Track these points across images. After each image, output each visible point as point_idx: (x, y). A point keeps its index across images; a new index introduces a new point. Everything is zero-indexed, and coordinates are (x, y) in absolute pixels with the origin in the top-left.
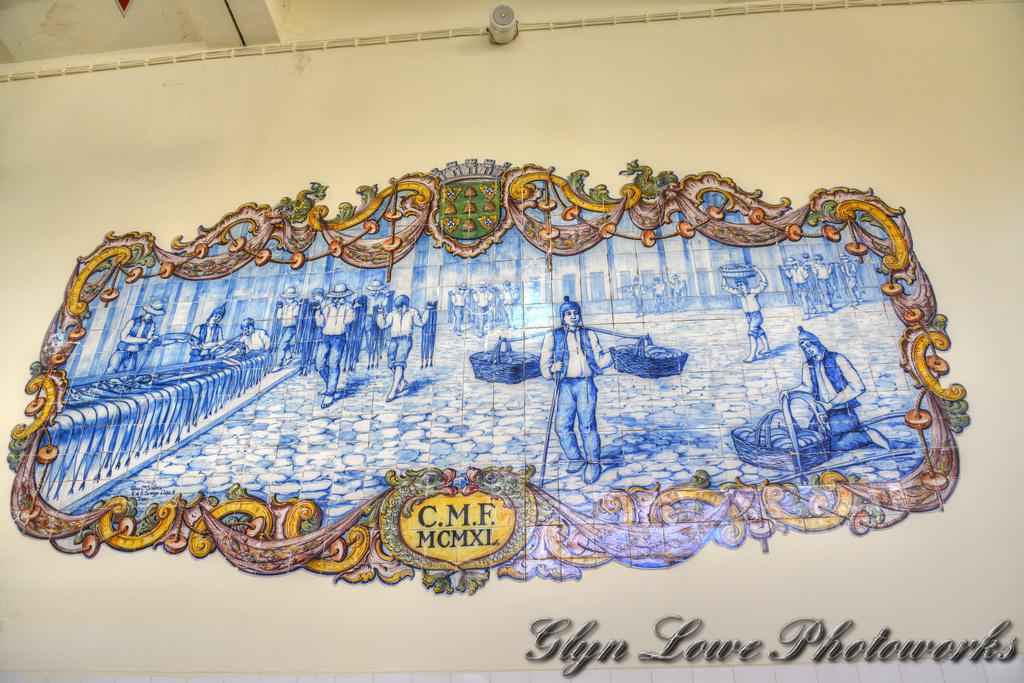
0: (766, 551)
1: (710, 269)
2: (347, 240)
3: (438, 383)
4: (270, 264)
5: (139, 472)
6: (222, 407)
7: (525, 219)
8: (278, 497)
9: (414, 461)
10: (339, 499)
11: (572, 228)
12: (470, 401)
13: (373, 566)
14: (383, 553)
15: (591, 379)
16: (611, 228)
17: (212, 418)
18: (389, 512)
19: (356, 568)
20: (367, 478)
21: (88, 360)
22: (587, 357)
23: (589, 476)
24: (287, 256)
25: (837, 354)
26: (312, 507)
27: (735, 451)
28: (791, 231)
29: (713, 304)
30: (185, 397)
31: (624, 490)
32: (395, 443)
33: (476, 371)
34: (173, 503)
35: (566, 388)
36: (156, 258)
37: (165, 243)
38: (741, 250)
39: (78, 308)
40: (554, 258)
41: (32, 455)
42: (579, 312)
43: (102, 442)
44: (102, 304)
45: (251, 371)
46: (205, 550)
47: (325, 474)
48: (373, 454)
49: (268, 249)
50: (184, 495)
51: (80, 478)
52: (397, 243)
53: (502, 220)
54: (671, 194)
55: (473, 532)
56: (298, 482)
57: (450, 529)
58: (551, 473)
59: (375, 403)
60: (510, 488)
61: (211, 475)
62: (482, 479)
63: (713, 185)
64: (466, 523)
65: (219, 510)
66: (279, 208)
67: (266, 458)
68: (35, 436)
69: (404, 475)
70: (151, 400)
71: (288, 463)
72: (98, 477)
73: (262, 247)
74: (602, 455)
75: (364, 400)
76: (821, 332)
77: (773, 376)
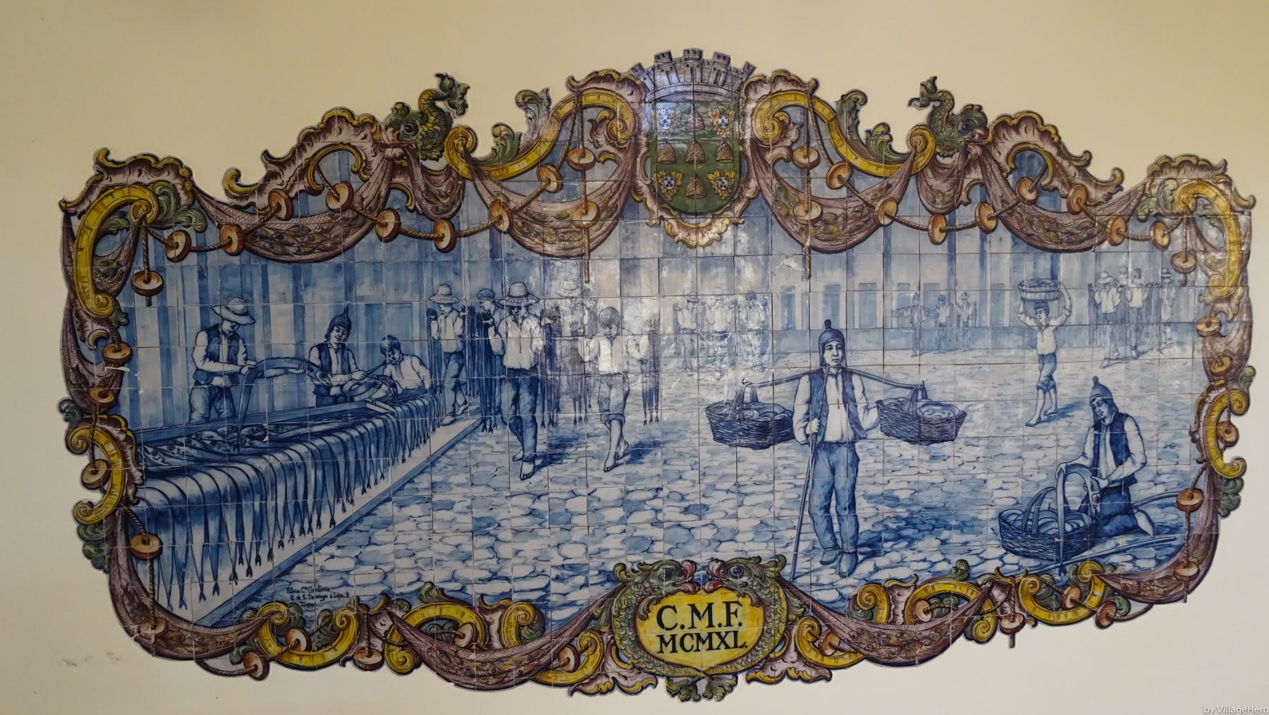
0: (1013, 645)
1: (1007, 285)
2: (516, 201)
3: (668, 445)
4: (401, 239)
5: (293, 567)
6: (383, 476)
7: (775, 181)
8: (485, 598)
9: (647, 551)
10: (562, 600)
11: (838, 204)
12: (708, 471)
13: (611, 675)
14: (620, 660)
15: (852, 444)
16: (891, 206)
17: (375, 492)
18: (623, 613)
19: (592, 679)
20: (592, 573)
21: (154, 399)
22: (849, 413)
23: (844, 568)
24: (428, 225)
25: (1127, 416)
26: (530, 610)
27: (999, 537)
28: (1114, 229)
29: (1005, 342)
30: (324, 459)
31: (880, 584)
32: (621, 527)
33: (714, 429)
34: (352, 610)
35: (823, 456)
36: (206, 216)
37: (212, 184)
38: (1049, 255)
39: (100, 305)
40: (816, 256)
41: (121, 547)
42: (842, 347)
43: (222, 527)
44: (140, 301)
45: (413, 423)
46: (408, 664)
47: (539, 569)
48: (596, 543)
49: (391, 209)
50: (362, 598)
51: (208, 578)
52: (592, 214)
53: (744, 178)
54: (976, 150)
55: (718, 634)
56: (507, 579)
57: (693, 631)
58: (802, 564)
59: (590, 473)
60: (758, 583)
61: (393, 570)
62: (726, 572)
63: (1029, 136)
64: (711, 625)
65: (415, 616)
66: (394, 124)
67: (461, 548)
68: (115, 520)
69: (636, 569)
70: (277, 465)
71: (491, 555)
72: (234, 577)
73: (381, 204)
74: (859, 542)
75: (574, 469)
76: (1115, 386)
77: (1055, 444)
